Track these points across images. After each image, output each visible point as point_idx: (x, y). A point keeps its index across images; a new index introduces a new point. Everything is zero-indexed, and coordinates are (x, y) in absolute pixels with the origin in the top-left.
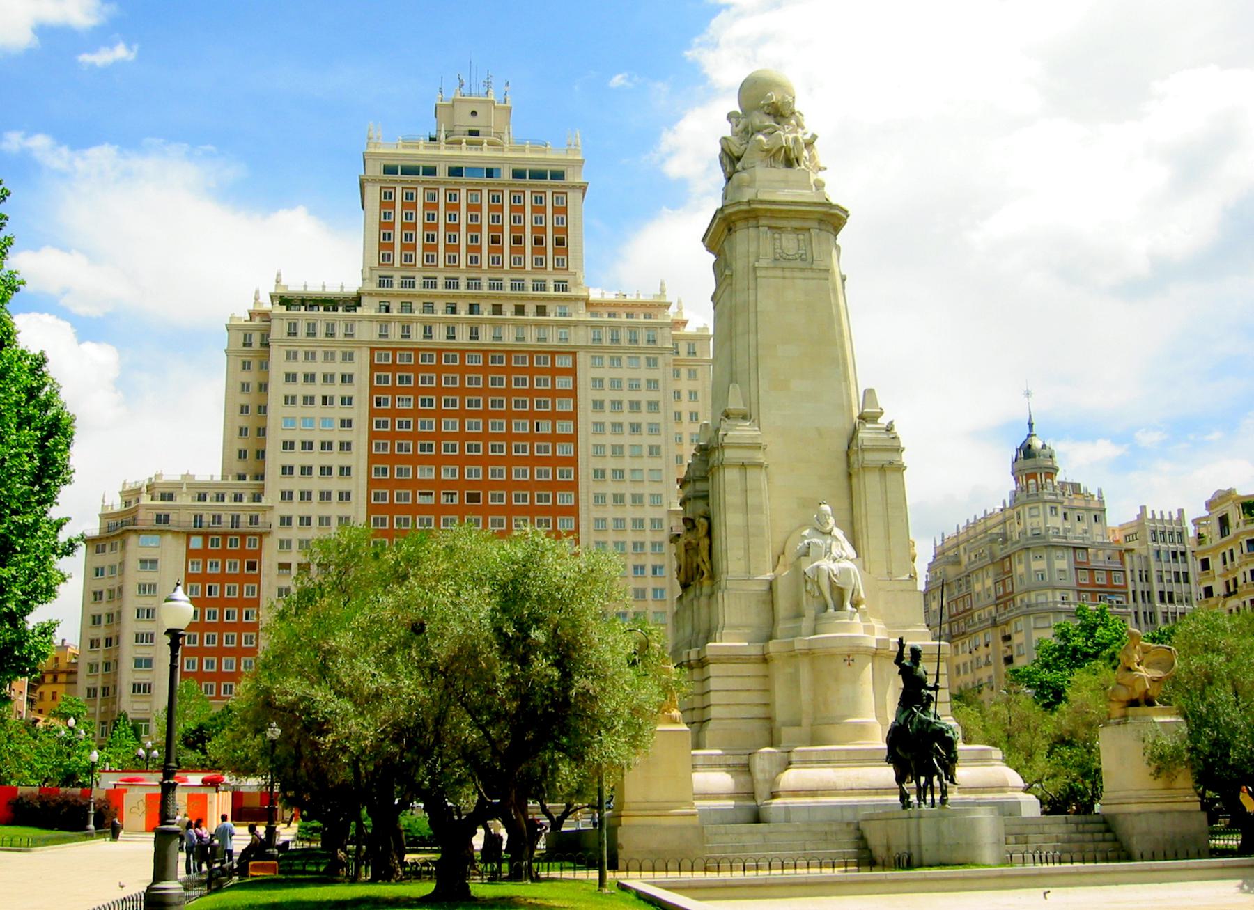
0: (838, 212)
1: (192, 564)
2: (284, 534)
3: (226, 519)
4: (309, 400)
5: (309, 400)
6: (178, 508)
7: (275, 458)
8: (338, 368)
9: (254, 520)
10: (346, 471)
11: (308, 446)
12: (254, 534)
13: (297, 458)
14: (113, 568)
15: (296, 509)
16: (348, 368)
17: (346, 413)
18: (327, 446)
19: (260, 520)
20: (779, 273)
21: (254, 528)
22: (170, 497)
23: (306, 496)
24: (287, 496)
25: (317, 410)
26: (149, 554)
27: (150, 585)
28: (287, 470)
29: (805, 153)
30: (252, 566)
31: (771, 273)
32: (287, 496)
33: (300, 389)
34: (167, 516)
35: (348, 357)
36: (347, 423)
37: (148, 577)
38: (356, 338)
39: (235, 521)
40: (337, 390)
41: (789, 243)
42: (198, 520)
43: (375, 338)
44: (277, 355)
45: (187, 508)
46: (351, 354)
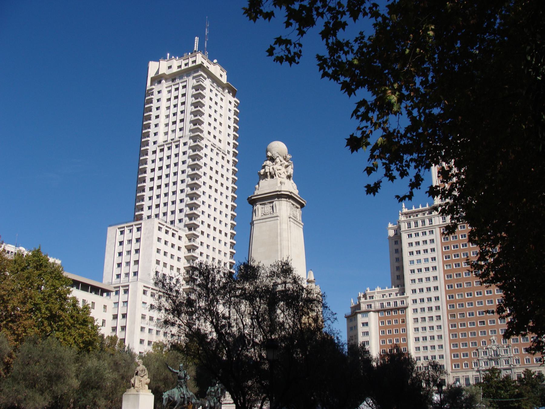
0: (283, 193)
1: (381, 322)
2: (415, 306)
3: (392, 303)
4: (418, 252)
5: (418, 252)
6: (374, 302)
7: (408, 277)
8: (428, 237)
9: (402, 302)
10: (435, 278)
11: (420, 270)
12: (403, 308)
13: (417, 276)
14: (355, 327)
15: (418, 296)
16: (432, 237)
17: (434, 255)
18: (427, 269)
19: (405, 302)
20: (261, 221)
21: (402, 306)
22: (372, 297)
23: (421, 290)
24: (414, 291)
25: (422, 256)
26: (365, 320)
27: (366, 332)
28: (413, 281)
29: (283, 169)
30: (403, 321)
31: (259, 221)
32: (414, 291)
33: (414, 249)
34: (371, 305)
35: (431, 232)
36: (434, 259)
37: (365, 329)
38: (434, 224)
39: (396, 303)
40: (429, 246)
41: (268, 208)
42: (382, 304)
43: (441, 223)
44: (404, 236)
45: (378, 301)
46: (432, 231)
